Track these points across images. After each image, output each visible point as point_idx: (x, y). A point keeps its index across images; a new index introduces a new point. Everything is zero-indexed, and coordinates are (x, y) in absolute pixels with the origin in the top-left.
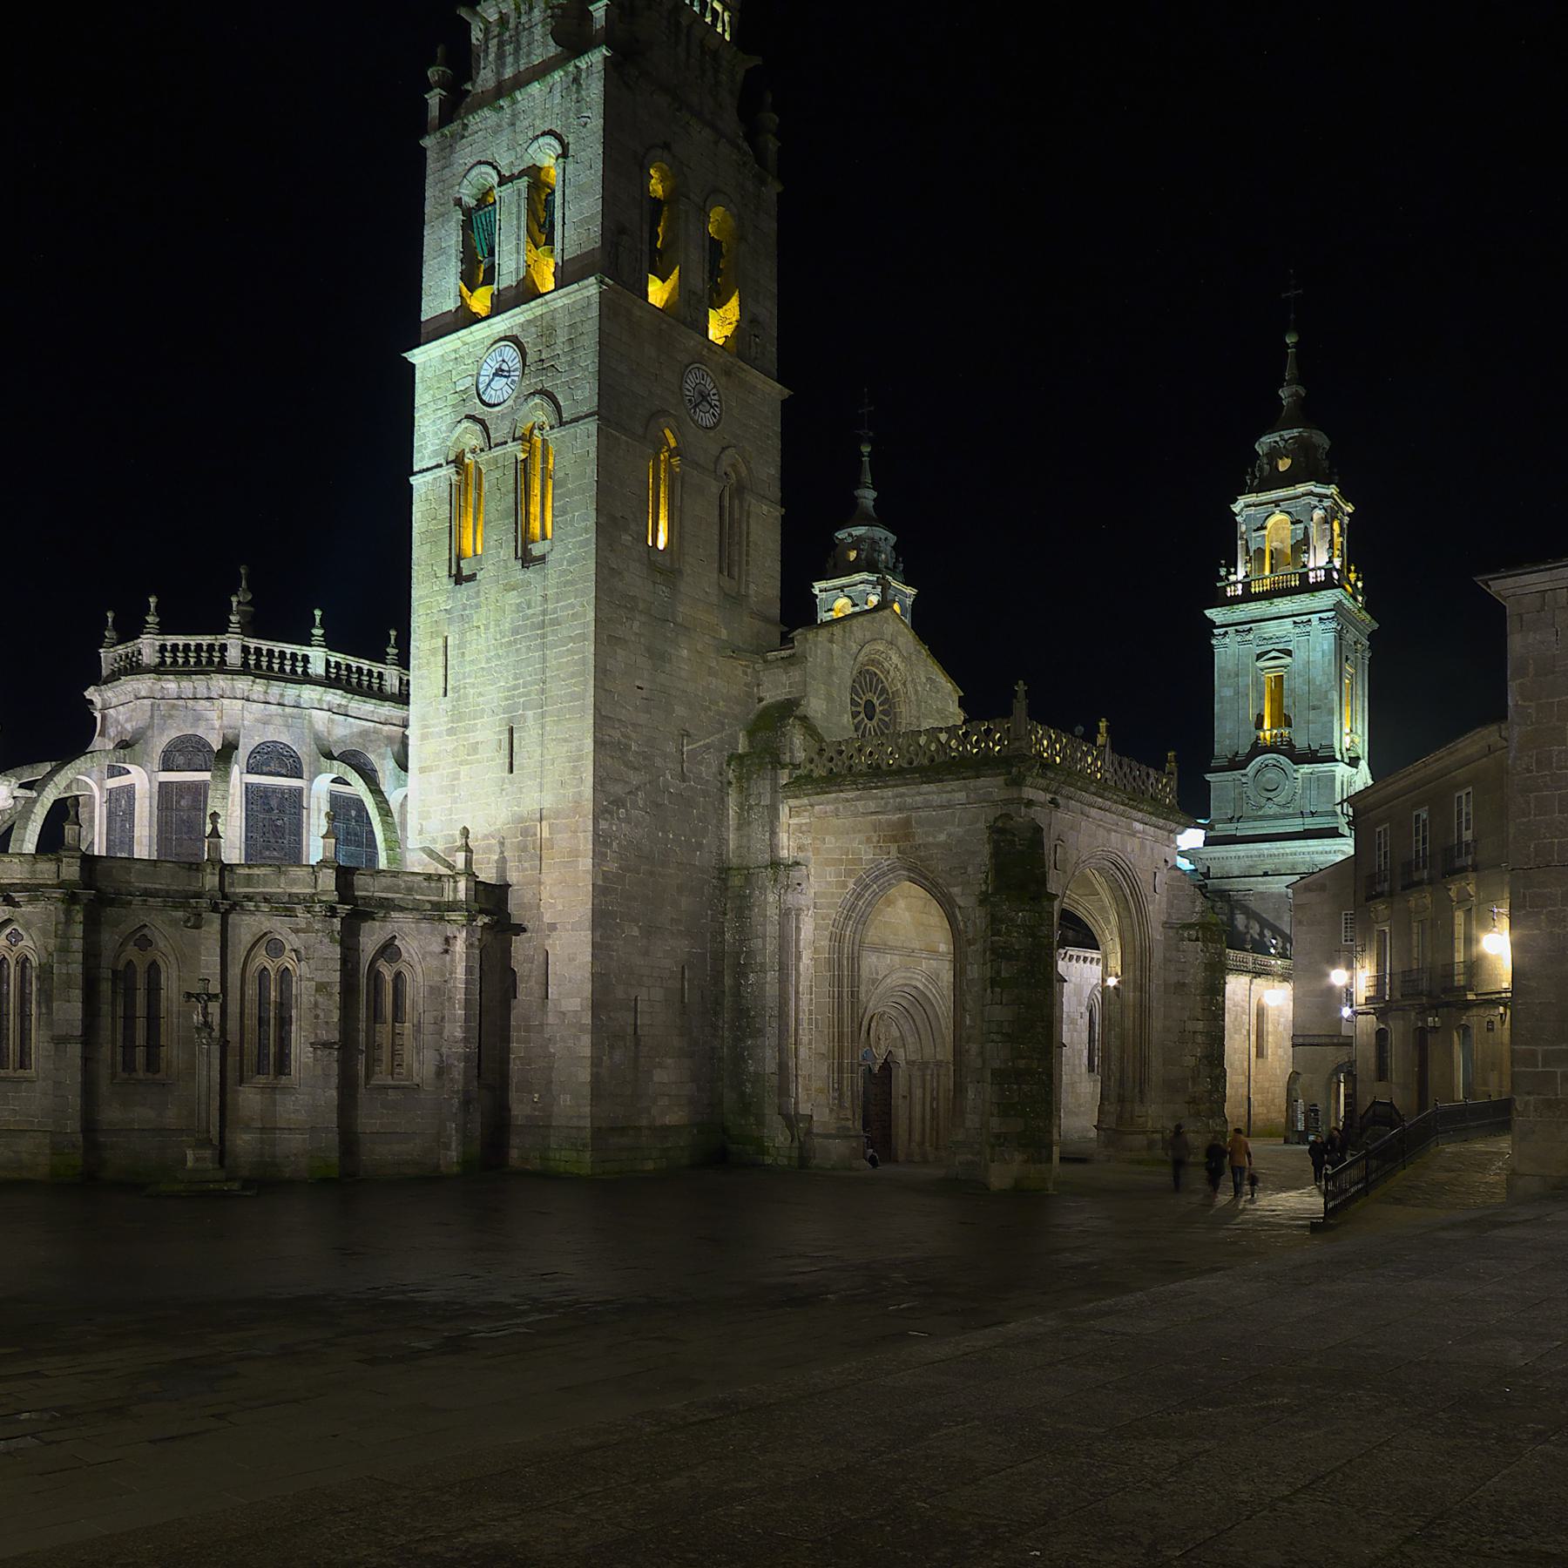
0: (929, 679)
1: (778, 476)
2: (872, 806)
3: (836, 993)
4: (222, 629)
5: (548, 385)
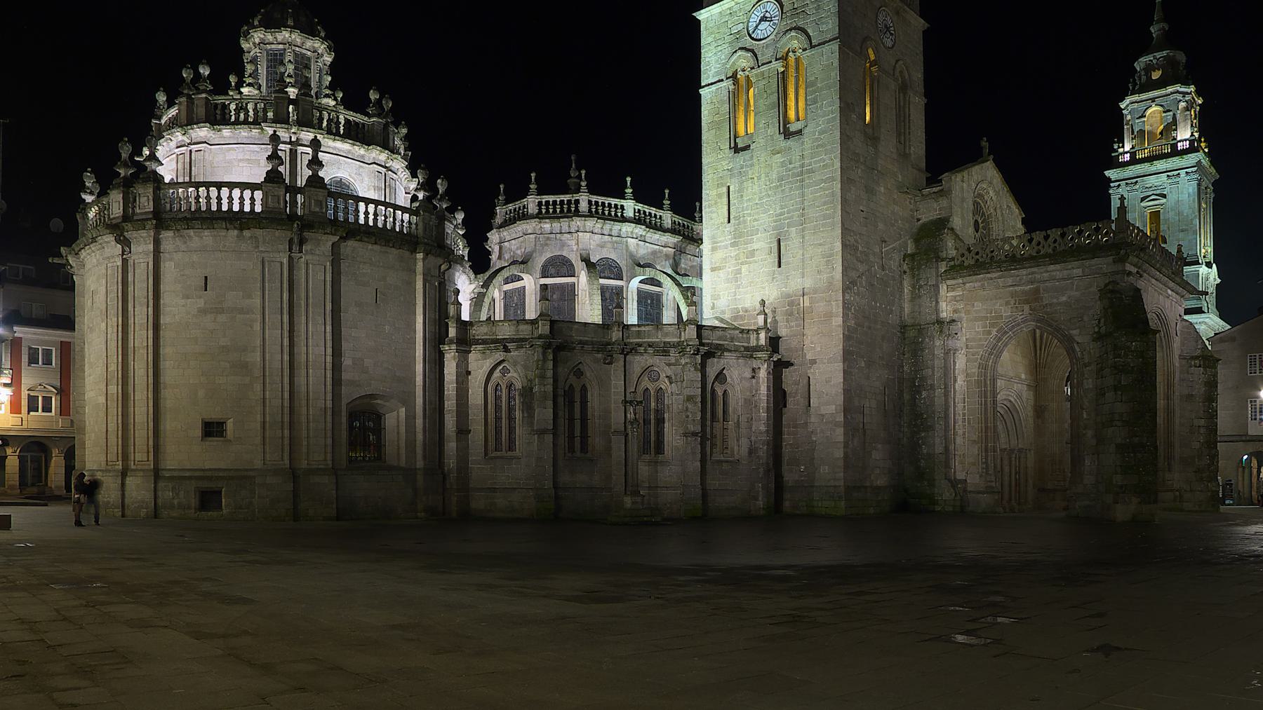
0: (1008, 206)
2: (1010, 281)
4: (578, 191)
5: (800, 24)
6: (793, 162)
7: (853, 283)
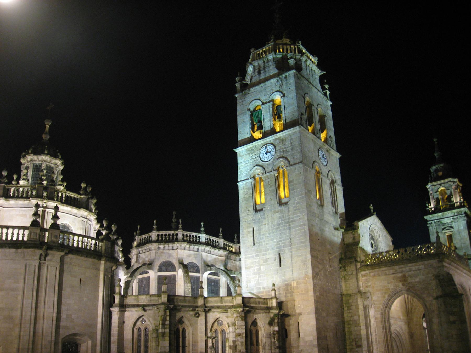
1: (340, 178)
2: (391, 272)
3: (385, 332)
4: (177, 229)
6: (285, 216)
7: (317, 274)
